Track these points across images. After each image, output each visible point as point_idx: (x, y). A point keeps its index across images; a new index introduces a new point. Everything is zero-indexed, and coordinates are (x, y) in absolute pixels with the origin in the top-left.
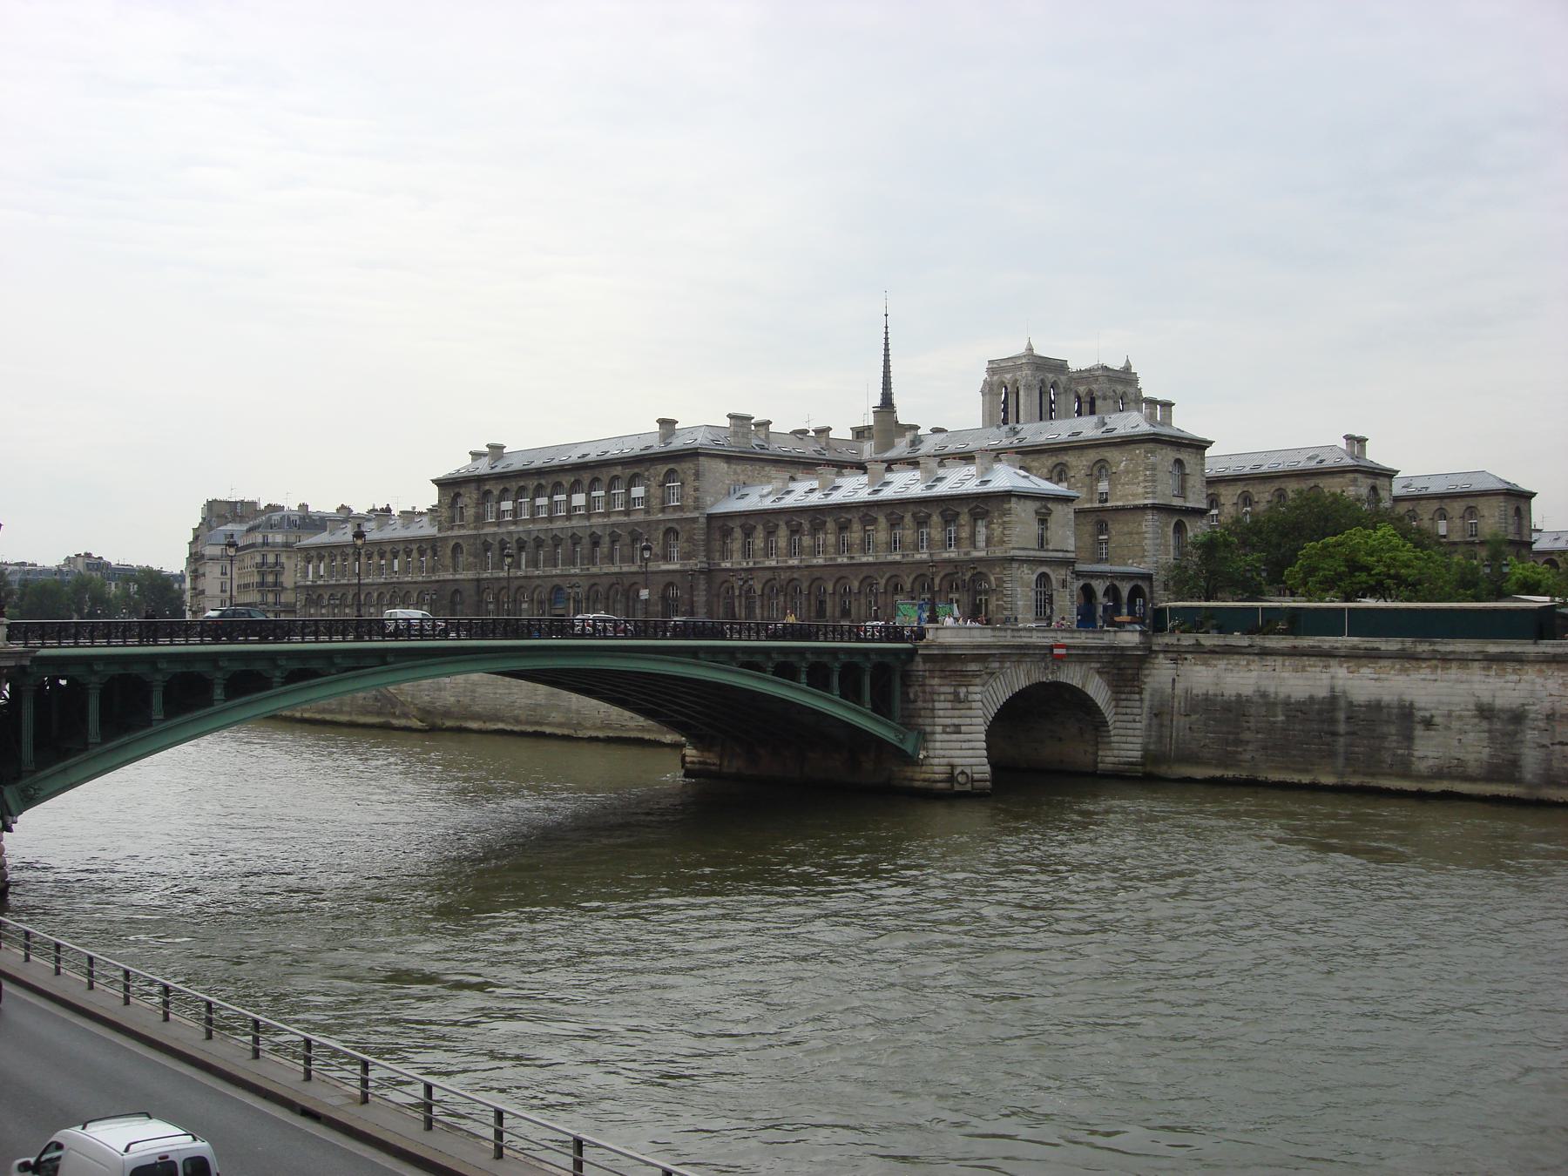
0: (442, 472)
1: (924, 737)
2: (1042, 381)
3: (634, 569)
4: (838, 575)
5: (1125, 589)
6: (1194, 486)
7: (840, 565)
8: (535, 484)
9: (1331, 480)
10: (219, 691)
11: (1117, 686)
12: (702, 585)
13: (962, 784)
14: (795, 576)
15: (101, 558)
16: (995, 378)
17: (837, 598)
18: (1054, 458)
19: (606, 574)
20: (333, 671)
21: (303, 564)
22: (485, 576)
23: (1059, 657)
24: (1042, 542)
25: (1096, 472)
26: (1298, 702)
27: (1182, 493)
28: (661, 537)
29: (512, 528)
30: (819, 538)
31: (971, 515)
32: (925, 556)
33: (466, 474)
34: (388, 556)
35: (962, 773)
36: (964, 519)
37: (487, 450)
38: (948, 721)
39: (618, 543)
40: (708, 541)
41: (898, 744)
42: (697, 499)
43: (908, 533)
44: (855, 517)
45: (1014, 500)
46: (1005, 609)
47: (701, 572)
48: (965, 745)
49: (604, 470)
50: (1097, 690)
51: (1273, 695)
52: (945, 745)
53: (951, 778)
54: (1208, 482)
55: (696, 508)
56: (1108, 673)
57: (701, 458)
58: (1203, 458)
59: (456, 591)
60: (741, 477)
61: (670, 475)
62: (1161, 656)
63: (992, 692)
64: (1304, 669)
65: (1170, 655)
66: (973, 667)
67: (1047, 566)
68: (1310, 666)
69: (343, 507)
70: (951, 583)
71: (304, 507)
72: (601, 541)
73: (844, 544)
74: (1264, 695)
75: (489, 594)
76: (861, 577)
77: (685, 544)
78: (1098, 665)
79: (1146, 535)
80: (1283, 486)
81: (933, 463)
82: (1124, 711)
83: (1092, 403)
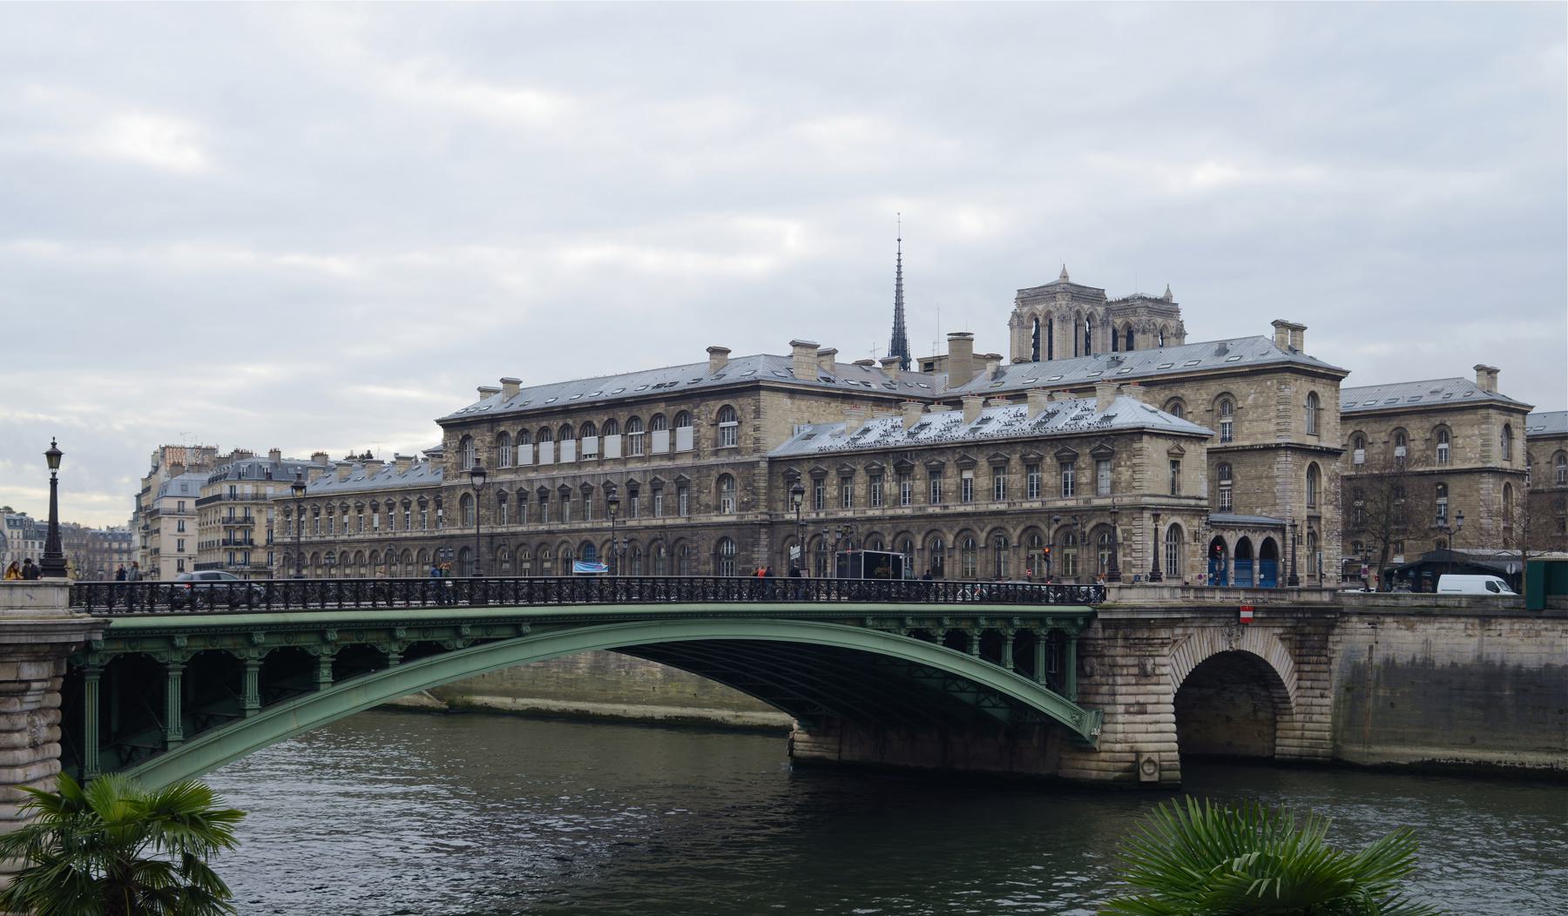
0: (446, 413)
1: (1104, 719)
2: (1078, 313)
3: (679, 521)
4: (928, 528)
5: (1257, 541)
6: (1328, 423)
7: (931, 516)
8: (561, 424)
9: (1459, 417)
10: (326, 672)
11: (1299, 656)
12: (764, 539)
13: (1148, 774)
14: (876, 528)
15: (24, 514)
16: (1025, 309)
17: (927, 553)
18: (1167, 392)
19: (647, 528)
20: (459, 644)
21: (280, 518)
22: (499, 530)
23: (1248, 619)
24: (1174, 486)
25: (1218, 407)
26: (1530, 672)
27: (1315, 430)
28: (713, 485)
29: (532, 475)
30: (905, 485)
31: (1094, 456)
32: (1036, 505)
33: (476, 413)
34: (383, 508)
35: (1149, 761)
36: (1085, 461)
37: (501, 386)
38: (1132, 699)
39: (660, 492)
40: (771, 487)
41: (1073, 727)
42: (757, 440)
43: (1015, 478)
44: (950, 461)
45: (1145, 438)
46: (1134, 566)
47: (761, 525)
48: (1152, 728)
49: (645, 407)
50: (1279, 659)
51: (1498, 664)
52: (1128, 728)
53: (1135, 768)
54: (1342, 418)
55: (756, 450)
56: (1290, 639)
57: (762, 392)
58: (1337, 390)
59: (465, 549)
60: (806, 415)
61: (725, 413)
62: (1354, 619)
63: (1175, 664)
64: (1538, 634)
65: (1371, 619)
66: (1164, 633)
67: (1179, 515)
68: (1546, 629)
69: (317, 455)
70: (1069, 536)
71: (275, 453)
72: (640, 490)
73: (935, 491)
75: (504, 551)
76: (957, 530)
77: (742, 493)
78: (1281, 631)
79: (1278, 480)
80: (1403, 424)
81: (1042, 397)
83: (1130, 337)
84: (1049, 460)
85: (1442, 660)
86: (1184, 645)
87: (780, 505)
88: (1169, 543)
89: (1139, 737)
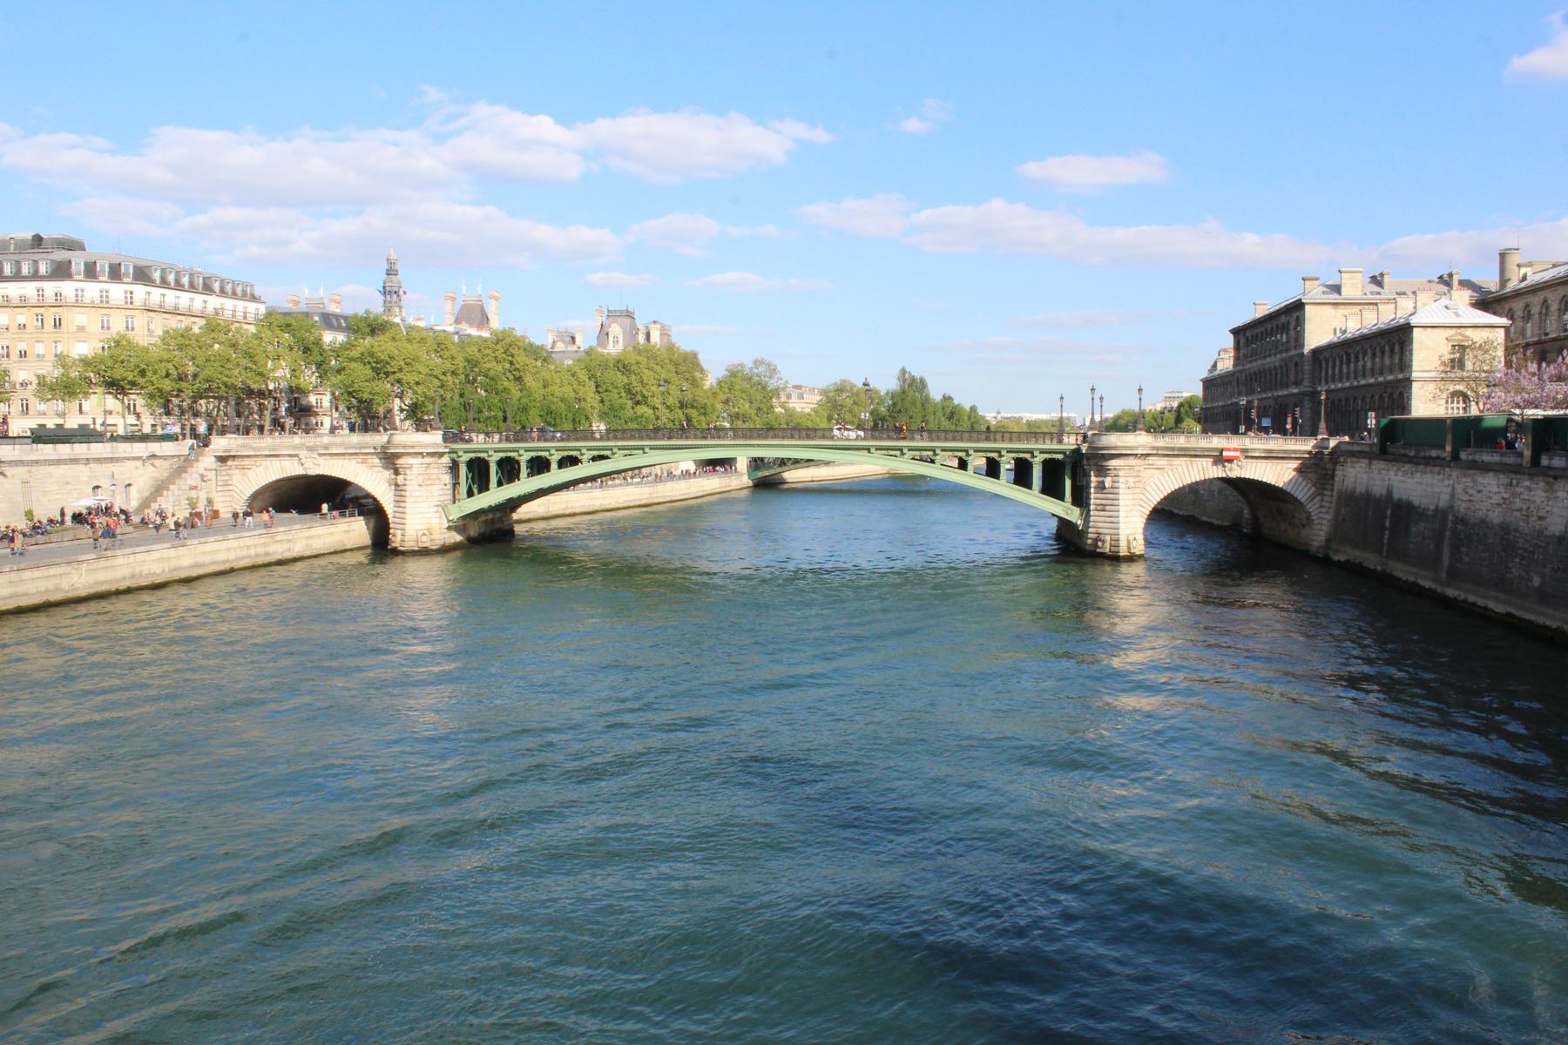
38: (1099, 502)
44: (1358, 348)
47: (1303, 394)
48: (1107, 519)
52: (1097, 519)
74: (1367, 491)
82: (1324, 503)
84: (1387, 348)
85: (1358, 491)
86: (1170, 472)
87: (1317, 381)
88: (1450, 406)
89: (1101, 525)
